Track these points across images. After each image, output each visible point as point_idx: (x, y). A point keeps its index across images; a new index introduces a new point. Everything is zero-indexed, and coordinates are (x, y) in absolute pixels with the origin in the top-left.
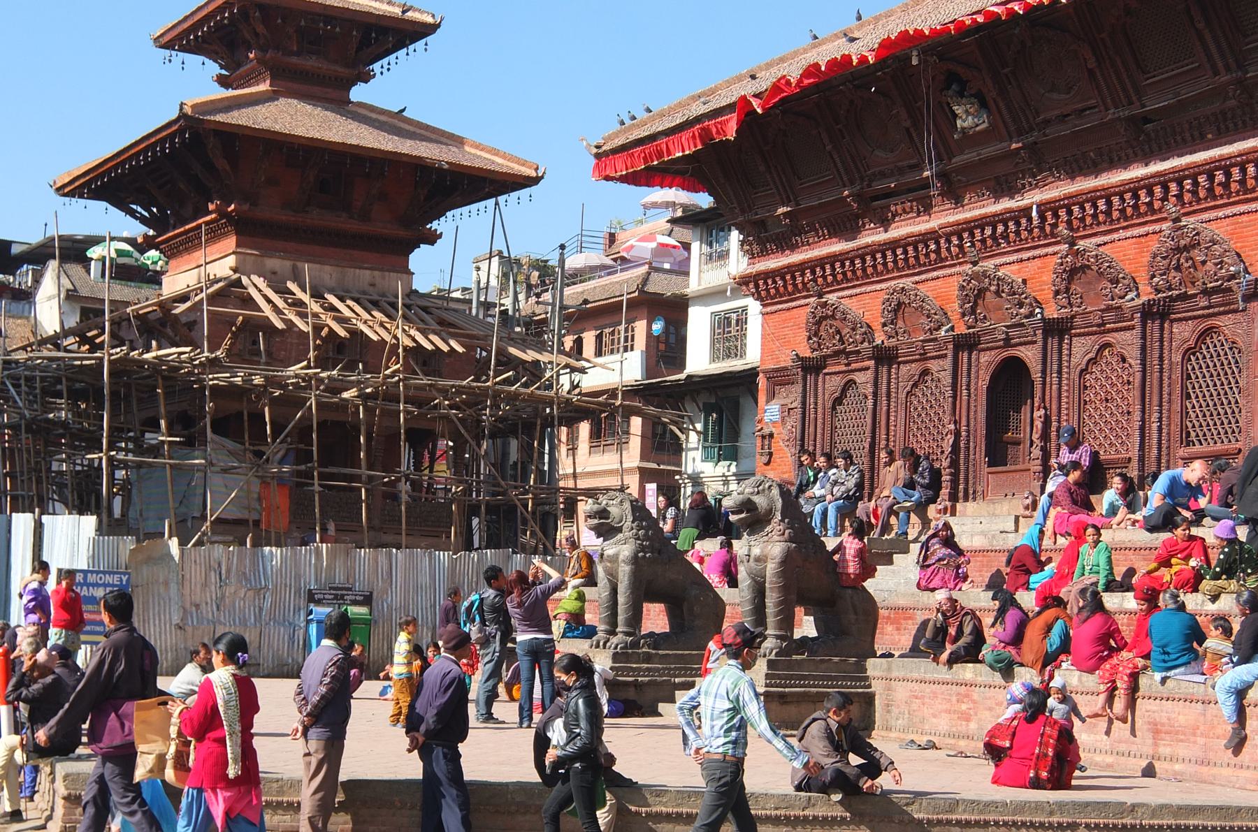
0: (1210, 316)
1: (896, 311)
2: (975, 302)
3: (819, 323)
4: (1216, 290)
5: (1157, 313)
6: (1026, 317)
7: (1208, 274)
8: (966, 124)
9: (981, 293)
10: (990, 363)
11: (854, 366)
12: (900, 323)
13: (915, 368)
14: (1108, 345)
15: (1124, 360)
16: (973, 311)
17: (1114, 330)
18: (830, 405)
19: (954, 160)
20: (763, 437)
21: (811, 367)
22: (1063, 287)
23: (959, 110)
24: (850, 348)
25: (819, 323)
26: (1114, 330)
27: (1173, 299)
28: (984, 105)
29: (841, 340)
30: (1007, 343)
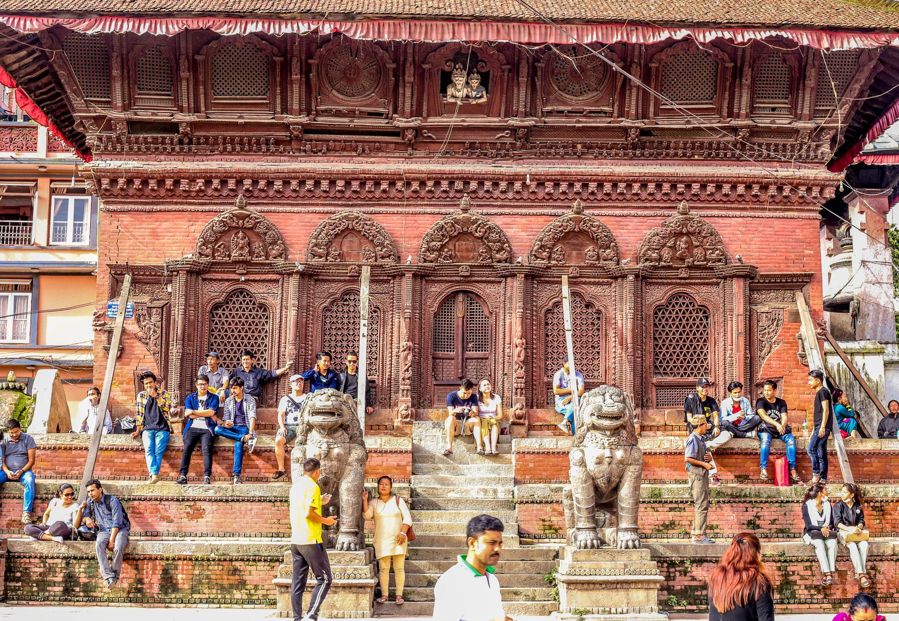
0: (683, 284)
1: (337, 235)
4: (698, 267)
5: (644, 279)
6: (499, 261)
8: (459, 94)
9: (462, 235)
10: (440, 294)
11: (252, 277)
12: (335, 246)
13: (337, 289)
17: (585, 283)
18: (208, 309)
19: (431, 119)
21: (196, 272)
22: (549, 244)
23: (459, 80)
24: (255, 260)
26: (585, 283)
27: (655, 268)
28: (484, 83)
29: (251, 253)
30: (467, 280)
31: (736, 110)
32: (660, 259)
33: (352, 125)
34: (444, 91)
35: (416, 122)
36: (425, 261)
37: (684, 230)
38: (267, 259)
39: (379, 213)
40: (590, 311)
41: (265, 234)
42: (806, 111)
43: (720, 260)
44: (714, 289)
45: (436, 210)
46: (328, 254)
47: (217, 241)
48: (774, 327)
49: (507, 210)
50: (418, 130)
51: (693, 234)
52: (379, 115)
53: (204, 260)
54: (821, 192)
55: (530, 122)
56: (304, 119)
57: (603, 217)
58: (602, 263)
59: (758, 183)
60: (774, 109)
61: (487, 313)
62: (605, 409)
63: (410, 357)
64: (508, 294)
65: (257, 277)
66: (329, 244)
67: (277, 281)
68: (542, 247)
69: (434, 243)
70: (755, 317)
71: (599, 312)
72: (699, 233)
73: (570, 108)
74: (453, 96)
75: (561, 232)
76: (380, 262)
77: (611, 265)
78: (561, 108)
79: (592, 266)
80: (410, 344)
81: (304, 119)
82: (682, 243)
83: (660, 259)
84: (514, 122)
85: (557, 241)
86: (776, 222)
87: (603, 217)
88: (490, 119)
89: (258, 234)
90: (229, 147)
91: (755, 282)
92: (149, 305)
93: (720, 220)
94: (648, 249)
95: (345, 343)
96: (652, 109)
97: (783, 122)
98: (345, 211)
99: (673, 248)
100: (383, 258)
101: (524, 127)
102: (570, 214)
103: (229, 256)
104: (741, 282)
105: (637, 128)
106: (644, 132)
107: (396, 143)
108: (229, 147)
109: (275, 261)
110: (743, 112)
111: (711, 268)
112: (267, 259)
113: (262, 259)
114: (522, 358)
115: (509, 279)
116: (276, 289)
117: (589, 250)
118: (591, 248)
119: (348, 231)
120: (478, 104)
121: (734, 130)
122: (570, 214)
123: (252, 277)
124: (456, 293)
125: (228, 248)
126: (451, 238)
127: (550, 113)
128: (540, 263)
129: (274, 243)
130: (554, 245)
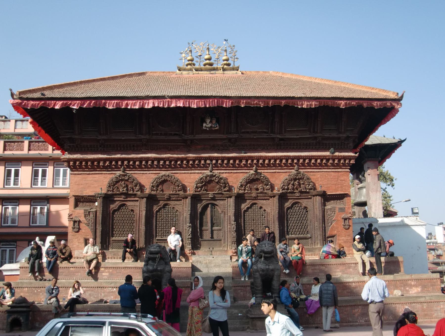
2: (205, 185)
3: (117, 182)
7: (302, 188)
9: (210, 181)
11: (128, 199)
12: (160, 186)
14: (255, 204)
15: (261, 208)
16: (201, 187)
19: (197, 136)
20: (75, 222)
23: (208, 121)
24: (129, 193)
25: (117, 182)
27: (287, 193)
28: (217, 122)
29: (127, 190)
31: (316, 130)
32: (288, 189)
33: (166, 139)
34: (202, 125)
35: (191, 137)
36: (196, 192)
37: (297, 177)
38: (133, 192)
39: (177, 173)
40: (261, 210)
41: (133, 182)
42: (343, 130)
43: (311, 189)
44: (310, 200)
45: (200, 172)
46: (157, 190)
47: (114, 185)
48: (333, 214)
49: (228, 171)
50: (192, 141)
51: (301, 179)
52: (177, 135)
53: (110, 193)
54: (350, 161)
55: (235, 136)
56: (147, 137)
57: (266, 173)
58: (265, 191)
59: (325, 158)
60: (330, 130)
61: (220, 212)
62: (266, 250)
63: (190, 230)
64: (229, 204)
65: (130, 199)
66: (158, 186)
67: (137, 201)
68: (242, 186)
69: (199, 185)
70: (326, 211)
71: (265, 210)
72: (303, 179)
73: (251, 131)
74: (205, 127)
75: (249, 179)
76: (178, 193)
77: (269, 192)
78: (248, 130)
79: (261, 193)
80: (190, 225)
81: (147, 137)
82: (296, 183)
83: (288, 189)
84: (230, 136)
85: (247, 183)
86: (332, 173)
87: (266, 173)
88: (220, 135)
89: (130, 182)
90: (119, 149)
91: (326, 198)
92: (89, 211)
93: (312, 173)
94: (284, 185)
95: (165, 225)
96: (283, 131)
97: (334, 135)
98: (163, 173)
99: (293, 185)
100: (179, 191)
101: (233, 138)
102: (252, 172)
103: (119, 191)
104: (320, 198)
105: (278, 138)
106: (281, 139)
107: (183, 146)
108: (119, 149)
109: (137, 193)
110: (319, 131)
111: (308, 193)
112: (133, 192)
113: (131, 192)
114: (235, 229)
115: (229, 199)
116: (137, 203)
117: (260, 186)
118: (261, 185)
119: (165, 181)
120: (215, 130)
121: (315, 138)
122: (252, 172)
123: (128, 199)
124: (209, 204)
125: (118, 188)
126: (206, 182)
127: (243, 133)
128: (241, 192)
129: (136, 186)
130: (247, 185)
